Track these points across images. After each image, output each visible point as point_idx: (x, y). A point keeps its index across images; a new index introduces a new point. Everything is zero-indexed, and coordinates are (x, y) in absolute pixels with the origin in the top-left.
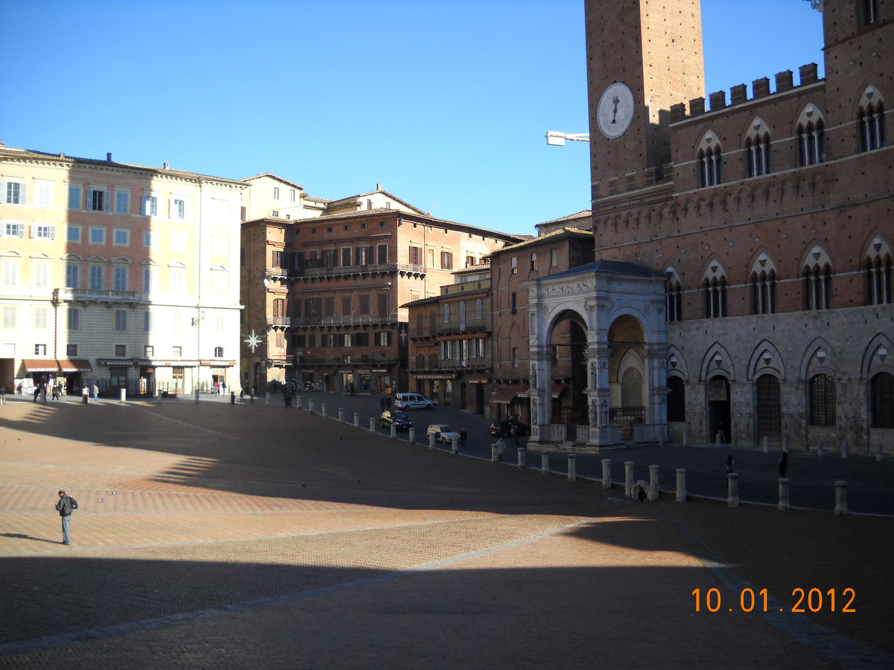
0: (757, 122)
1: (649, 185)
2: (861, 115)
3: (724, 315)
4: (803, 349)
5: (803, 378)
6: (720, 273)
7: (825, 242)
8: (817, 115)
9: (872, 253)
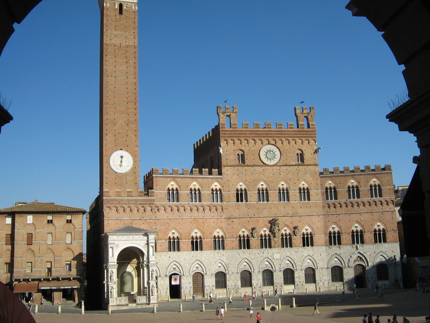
1: (140, 197)
4: (214, 263)
6: (176, 235)
7: (222, 229)
8: (218, 187)
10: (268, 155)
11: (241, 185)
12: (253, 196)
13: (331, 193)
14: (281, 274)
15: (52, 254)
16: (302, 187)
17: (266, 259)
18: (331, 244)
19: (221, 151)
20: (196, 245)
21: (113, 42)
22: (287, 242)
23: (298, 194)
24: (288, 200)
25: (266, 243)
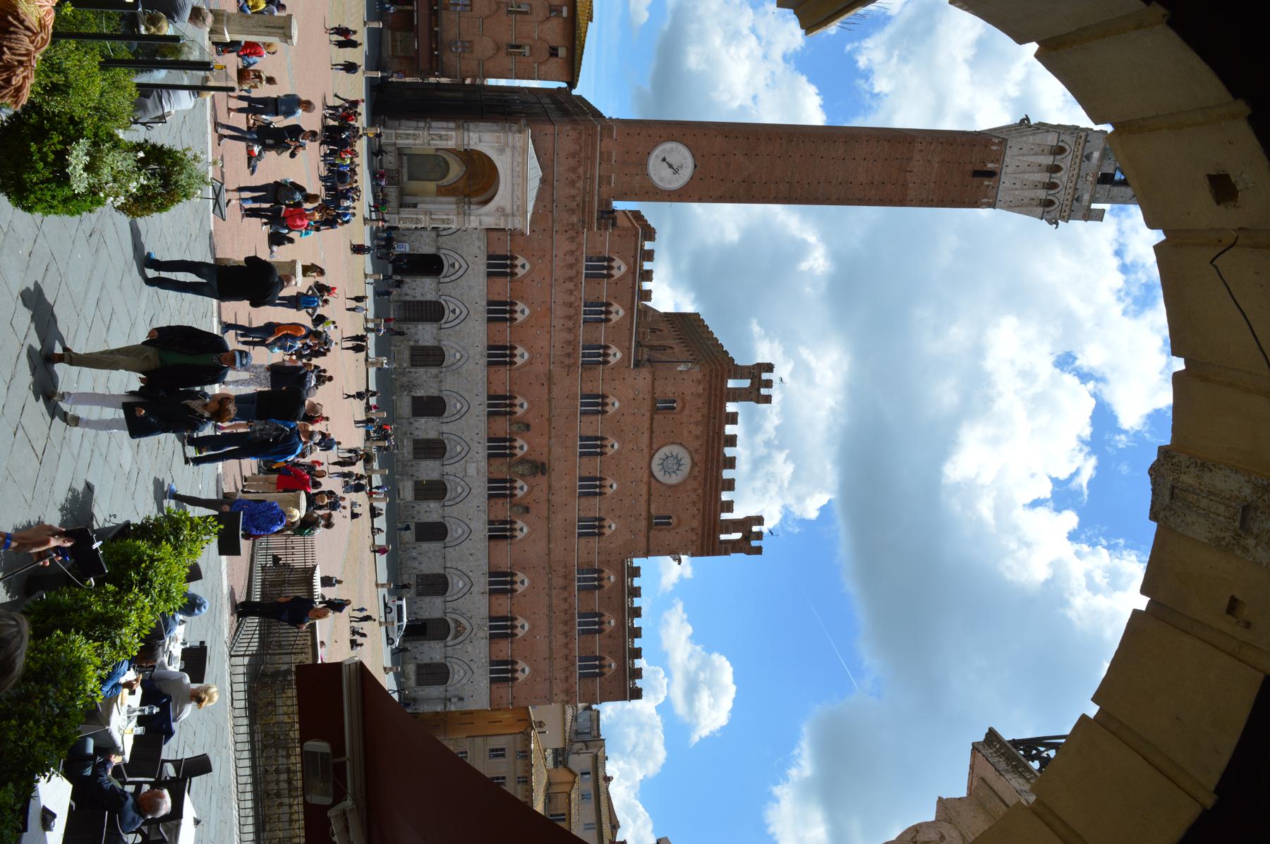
0: (621, 312)
2: (604, 397)
3: (490, 275)
5: (445, 342)
7: (530, 362)
8: (612, 360)
9: (518, 402)
10: (670, 461)
11: (614, 405)
12: (593, 426)
13: (592, 577)
14: (435, 476)
15: (487, 12)
16: (606, 523)
17: (466, 448)
18: (491, 574)
19: (681, 368)
20: (499, 312)
21: (917, 157)
22: (499, 489)
23: (591, 514)
24: (581, 495)
25: (499, 448)
